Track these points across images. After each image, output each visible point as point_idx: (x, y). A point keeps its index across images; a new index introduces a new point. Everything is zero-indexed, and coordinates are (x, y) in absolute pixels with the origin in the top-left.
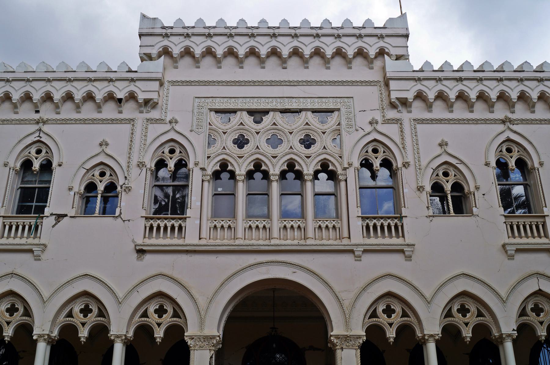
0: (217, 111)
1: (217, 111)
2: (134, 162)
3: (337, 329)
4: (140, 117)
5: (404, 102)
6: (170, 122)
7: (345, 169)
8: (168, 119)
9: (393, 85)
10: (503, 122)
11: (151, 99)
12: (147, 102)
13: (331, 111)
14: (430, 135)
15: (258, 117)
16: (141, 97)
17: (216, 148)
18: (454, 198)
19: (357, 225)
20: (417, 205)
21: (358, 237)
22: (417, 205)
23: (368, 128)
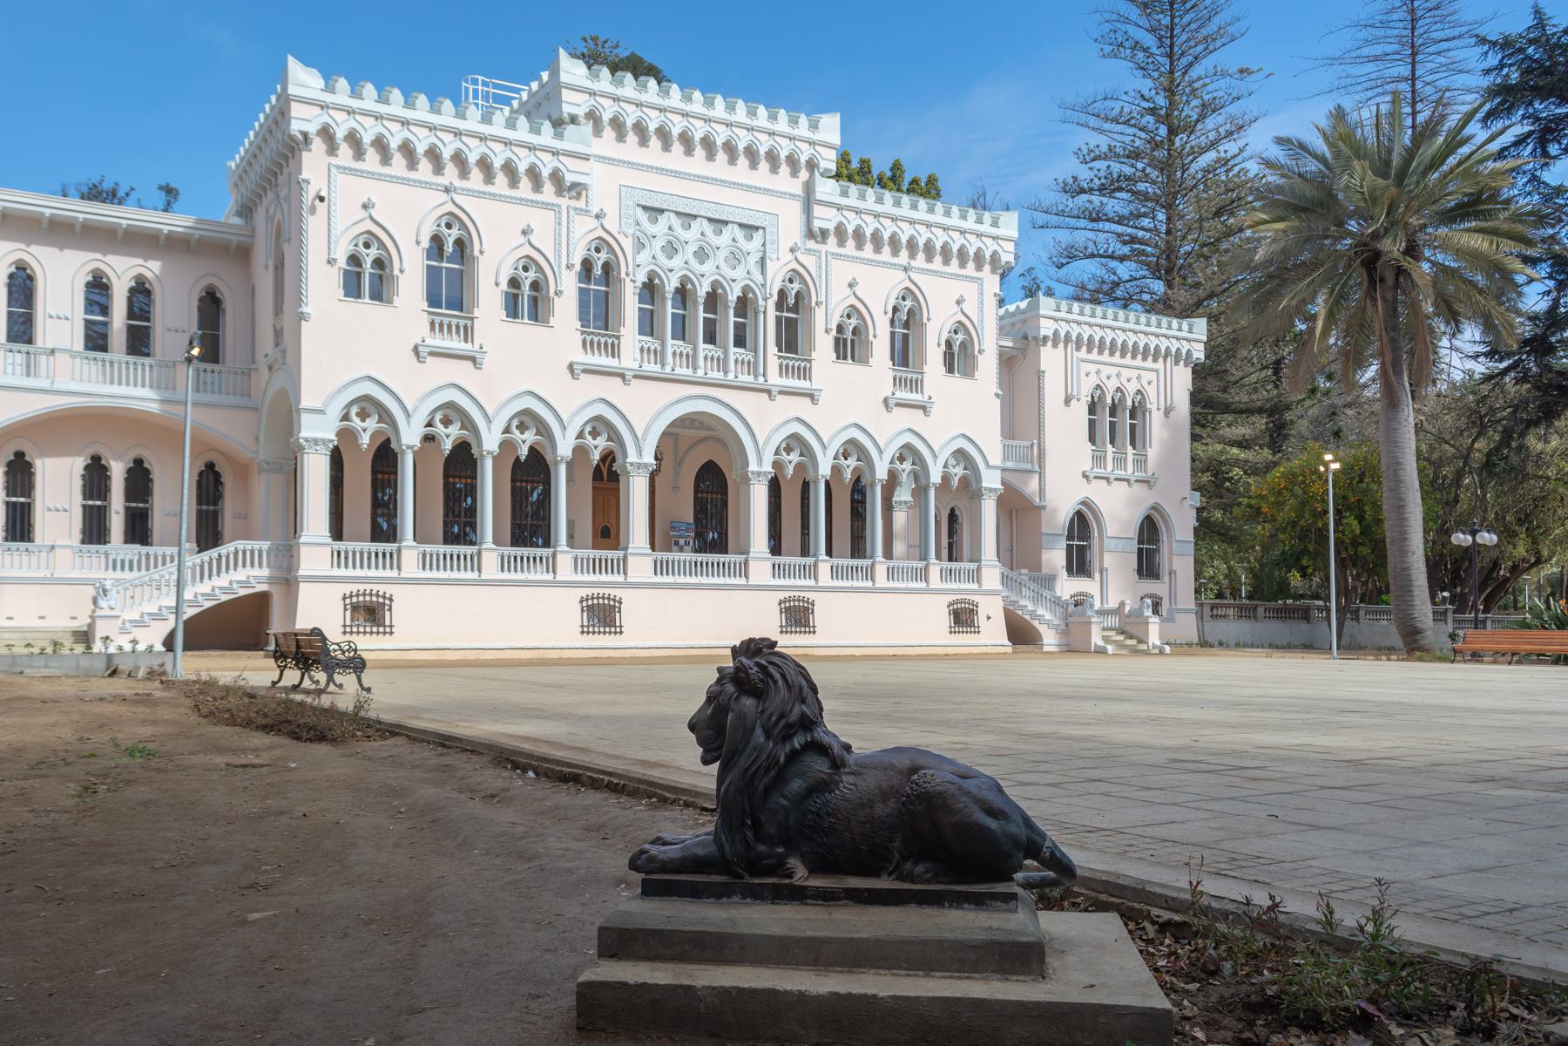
0: (645, 208)
1: (645, 208)
2: (564, 266)
3: (753, 467)
4: (564, 202)
5: (824, 233)
6: (597, 217)
7: (765, 299)
8: (596, 210)
9: (818, 211)
10: (906, 269)
11: (580, 184)
12: (574, 185)
13: (757, 228)
14: (841, 273)
15: (687, 220)
16: (569, 178)
17: (644, 257)
18: (850, 345)
19: (773, 363)
20: (823, 345)
21: (774, 379)
22: (823, 345)
23: (790, 256)
